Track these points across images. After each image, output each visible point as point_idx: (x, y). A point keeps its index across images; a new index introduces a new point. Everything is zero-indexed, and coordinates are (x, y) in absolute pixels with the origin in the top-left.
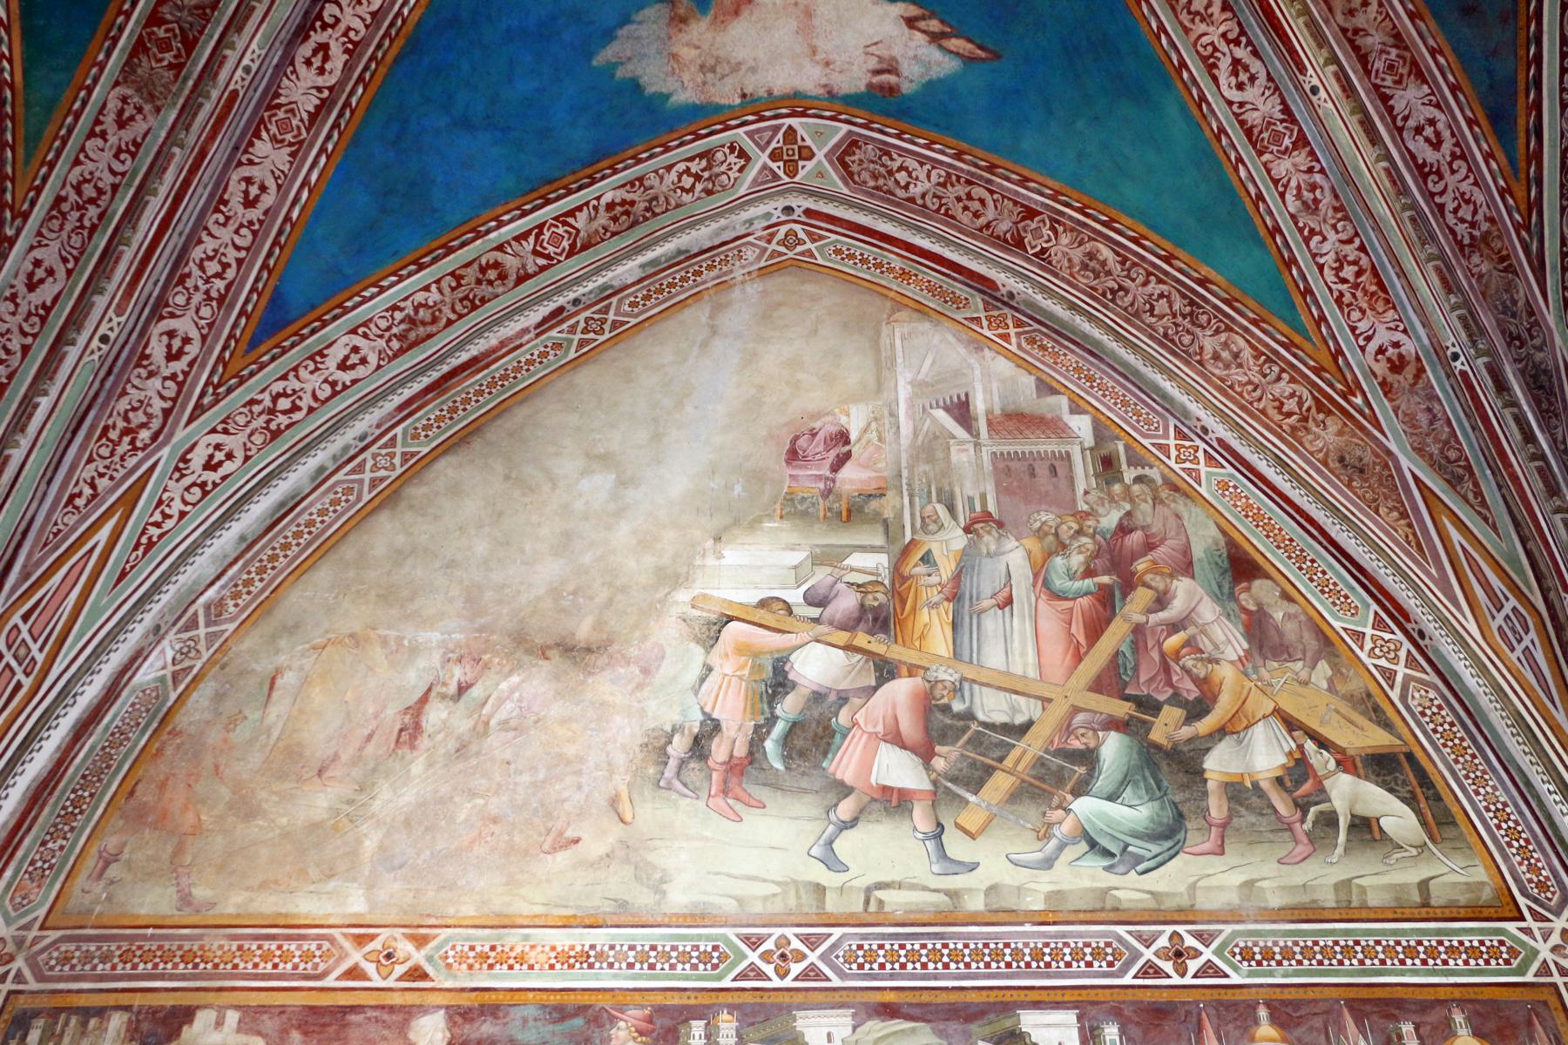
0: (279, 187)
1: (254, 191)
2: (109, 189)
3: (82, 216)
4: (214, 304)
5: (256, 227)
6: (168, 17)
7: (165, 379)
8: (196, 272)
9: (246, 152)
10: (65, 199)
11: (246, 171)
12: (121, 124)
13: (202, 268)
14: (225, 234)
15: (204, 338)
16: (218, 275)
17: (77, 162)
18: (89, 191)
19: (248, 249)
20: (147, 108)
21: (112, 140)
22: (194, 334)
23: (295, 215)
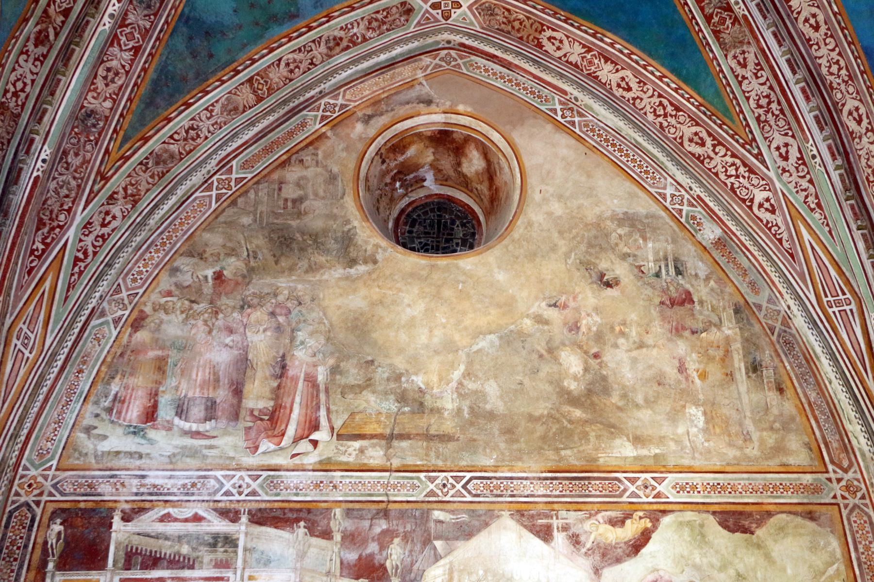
0: (818, 7)
1: (812, 21)
2: (769, 91)
3: (772, 112)
4: (850, 82)
5: (829, 33)
6: (711, 11)
7: (866, 134)
8: (832, 78)
9: (792, 12)
10: (760, 115)
11: (801, 19)
12: (744, 66)
13: (832, 74)
14: (824, 51)
15: (861, 100)
16: (840, 69)
17: (748, 98)
18: (763, 102)
19: (837, 46)
20: (745, 48)
21: (748, 74)
22: (857, 103)
23: (836, 9)
